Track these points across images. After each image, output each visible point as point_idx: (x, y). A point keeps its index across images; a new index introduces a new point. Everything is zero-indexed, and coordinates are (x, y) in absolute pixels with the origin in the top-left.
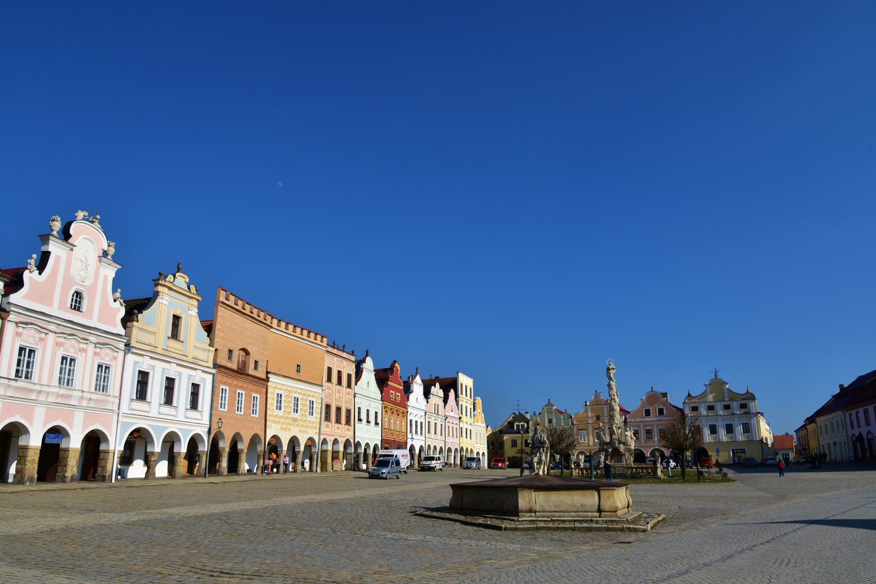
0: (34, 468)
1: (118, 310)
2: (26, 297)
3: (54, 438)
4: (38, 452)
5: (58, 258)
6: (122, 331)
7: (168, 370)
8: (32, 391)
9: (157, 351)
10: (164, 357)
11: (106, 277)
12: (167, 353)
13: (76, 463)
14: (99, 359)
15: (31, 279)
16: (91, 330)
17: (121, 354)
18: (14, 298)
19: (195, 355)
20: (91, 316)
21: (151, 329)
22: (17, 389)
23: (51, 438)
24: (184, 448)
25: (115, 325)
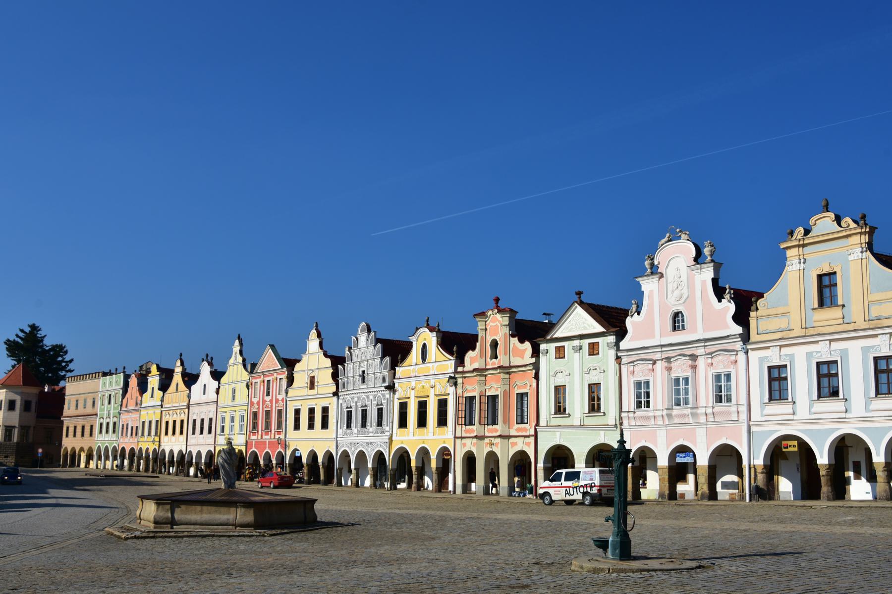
0: (665, 485)
1: (727, 308)
2: (631, 340)
3: (685, 457)
4: (667, 470)
5: (651, 292)
6: (739, 330)
7: (818, 352)
8: (648, 418)
9: (792, 334)
10: (809, 336)
11: (703, 283)
12: (812, 332)
13: (706, 480)
14: (713, 370)
15: (633, 323)
16: (692, 344)
17: (741, 356)
18: (624, 345)
19: (874, 314)
20: (695, 330)
21: (781, 310)
22: (641, 418)
23: (681, 457)
24: (878, 455)
25: (727, 327)
